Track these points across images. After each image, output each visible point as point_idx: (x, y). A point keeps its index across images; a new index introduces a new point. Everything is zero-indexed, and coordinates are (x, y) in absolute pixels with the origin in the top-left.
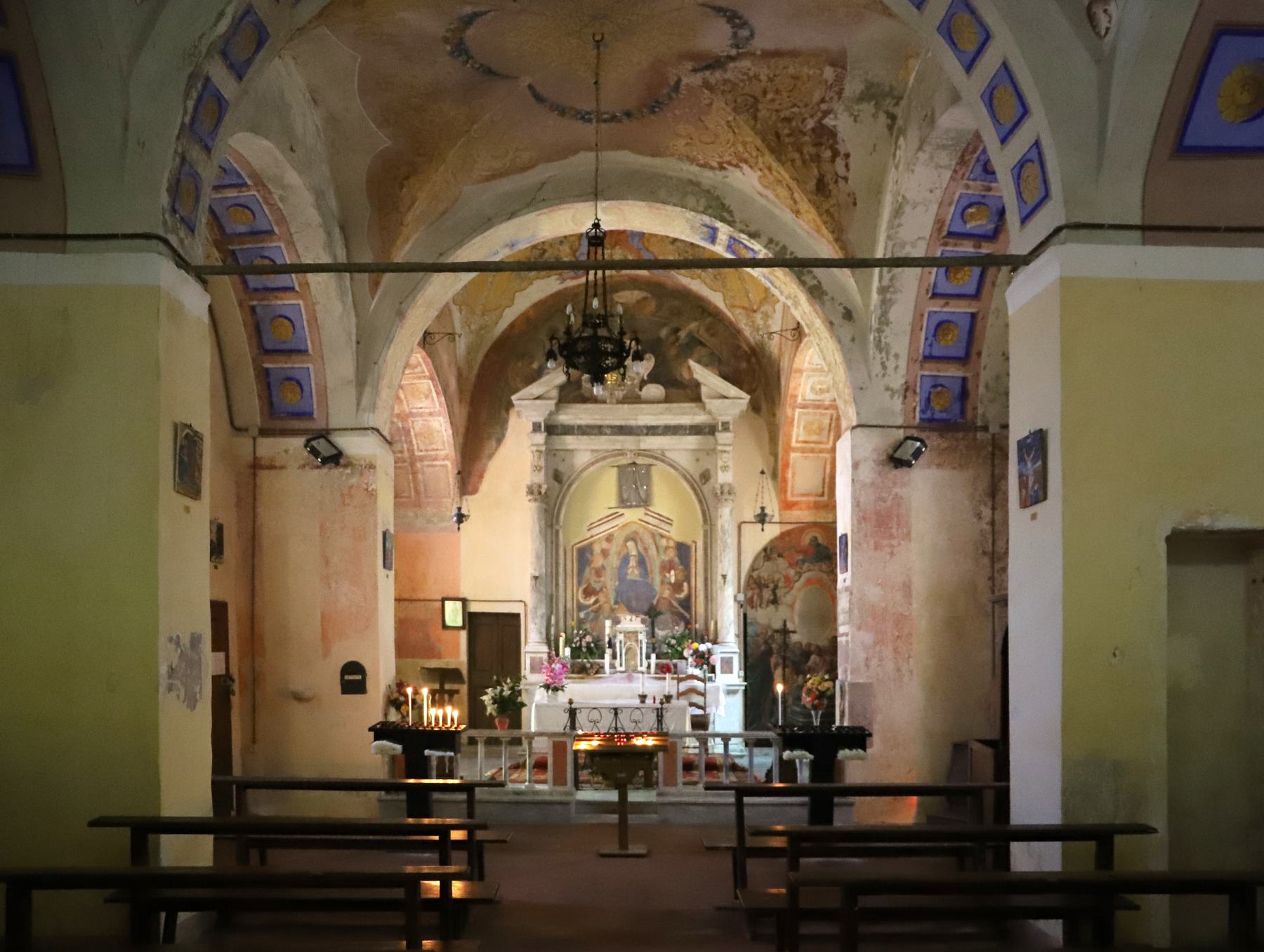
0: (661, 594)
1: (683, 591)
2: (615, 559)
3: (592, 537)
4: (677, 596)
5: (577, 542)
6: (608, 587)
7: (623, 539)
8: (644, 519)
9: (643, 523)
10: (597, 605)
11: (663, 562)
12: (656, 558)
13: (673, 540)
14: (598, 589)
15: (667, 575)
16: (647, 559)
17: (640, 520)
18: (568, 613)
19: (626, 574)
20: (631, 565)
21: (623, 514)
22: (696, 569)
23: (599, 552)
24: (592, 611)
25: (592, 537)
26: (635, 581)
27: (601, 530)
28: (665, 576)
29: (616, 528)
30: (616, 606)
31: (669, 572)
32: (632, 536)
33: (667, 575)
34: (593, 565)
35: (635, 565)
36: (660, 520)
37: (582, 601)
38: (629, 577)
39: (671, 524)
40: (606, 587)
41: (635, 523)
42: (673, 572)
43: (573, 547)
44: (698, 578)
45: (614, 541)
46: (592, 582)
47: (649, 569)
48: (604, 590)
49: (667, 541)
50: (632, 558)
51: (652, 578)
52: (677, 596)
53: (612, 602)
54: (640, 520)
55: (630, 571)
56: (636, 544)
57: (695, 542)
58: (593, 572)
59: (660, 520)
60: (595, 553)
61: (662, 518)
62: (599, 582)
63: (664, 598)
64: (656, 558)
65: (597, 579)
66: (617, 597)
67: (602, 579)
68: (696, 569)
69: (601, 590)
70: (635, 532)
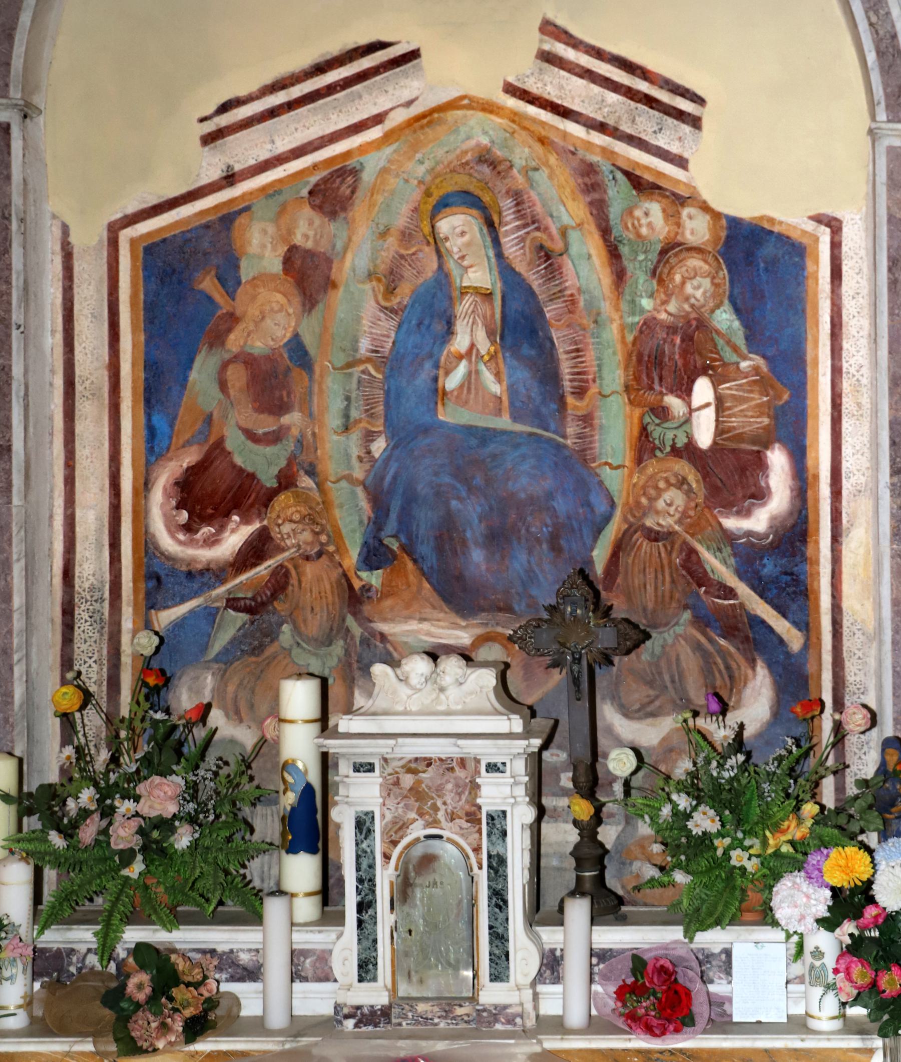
0: (636, 510)
1: (761, 495)
2: (369, 308)
3: (230, 179)
4: (731, 523)
5: (132, 208)
6: (331, 468)
7: (414, 194)
8: (533, 86)
9: (532, 110)
10: (262, 570)
11: (648, 325)
12: (606, 307)
13: (705, 208)
14: (268, 479)
15: (674, 402)
16: (550, 311)
17: (511, 90)
18: (81, 613)
19: (437, 394)
20: (460, 342)
21: (414, 55)
22: (837, 371)
23: (274, 263)
24: (232, 603)
25: (230, 179)
26: (485, 436)
27: (283, 145)
28: (662, 413)
29: (375, 133)
30: (375, 578)
31: (685, 391)
32: (462, 181)
33: (674, 402)
34: (235, 341)
35: (484, 346)
36: (630, 93)
37: (167, 542)
38: (449, 415)
39: (695, 122)
40: (311, 472)
41: (489, 108)
42: (703, 390)
43: (113, 243)
44: (847, 425)
45: (359, 210)
46: (234, 441)
47: (566, 368)
48: (305, 482)
49: (673, 217)
50: (464, 307)
51: (587, 419)
52: (731, 523)
53: (353, 554)
54: (511, 90)
55: (452, 382)
56: (491, 225)
57: (835, 226)
58: (237, 376)
59: (630, 93)
60: (247, 271)
61: (643, 86)
62: (275, 438)
63: (654, 536)
64: (606, 307)
65: (265, 424)
66: (377, 523)
67: (293, 419)
68: (837, 371)
69: (286, 481)
70: (486, 158)
